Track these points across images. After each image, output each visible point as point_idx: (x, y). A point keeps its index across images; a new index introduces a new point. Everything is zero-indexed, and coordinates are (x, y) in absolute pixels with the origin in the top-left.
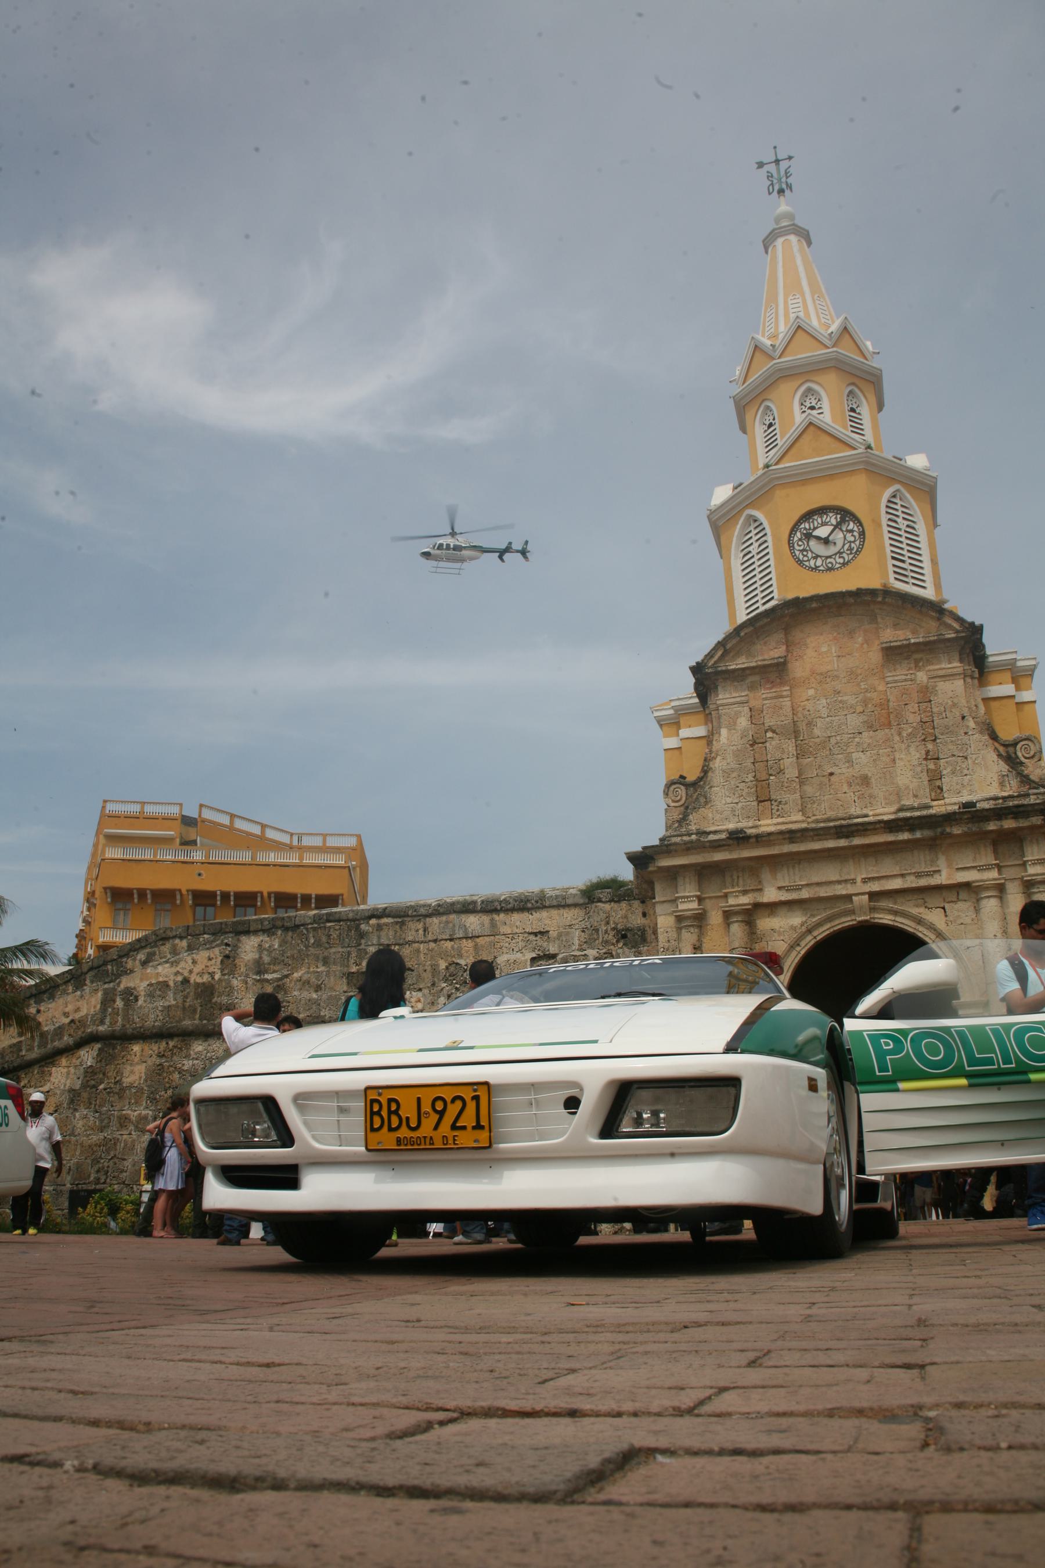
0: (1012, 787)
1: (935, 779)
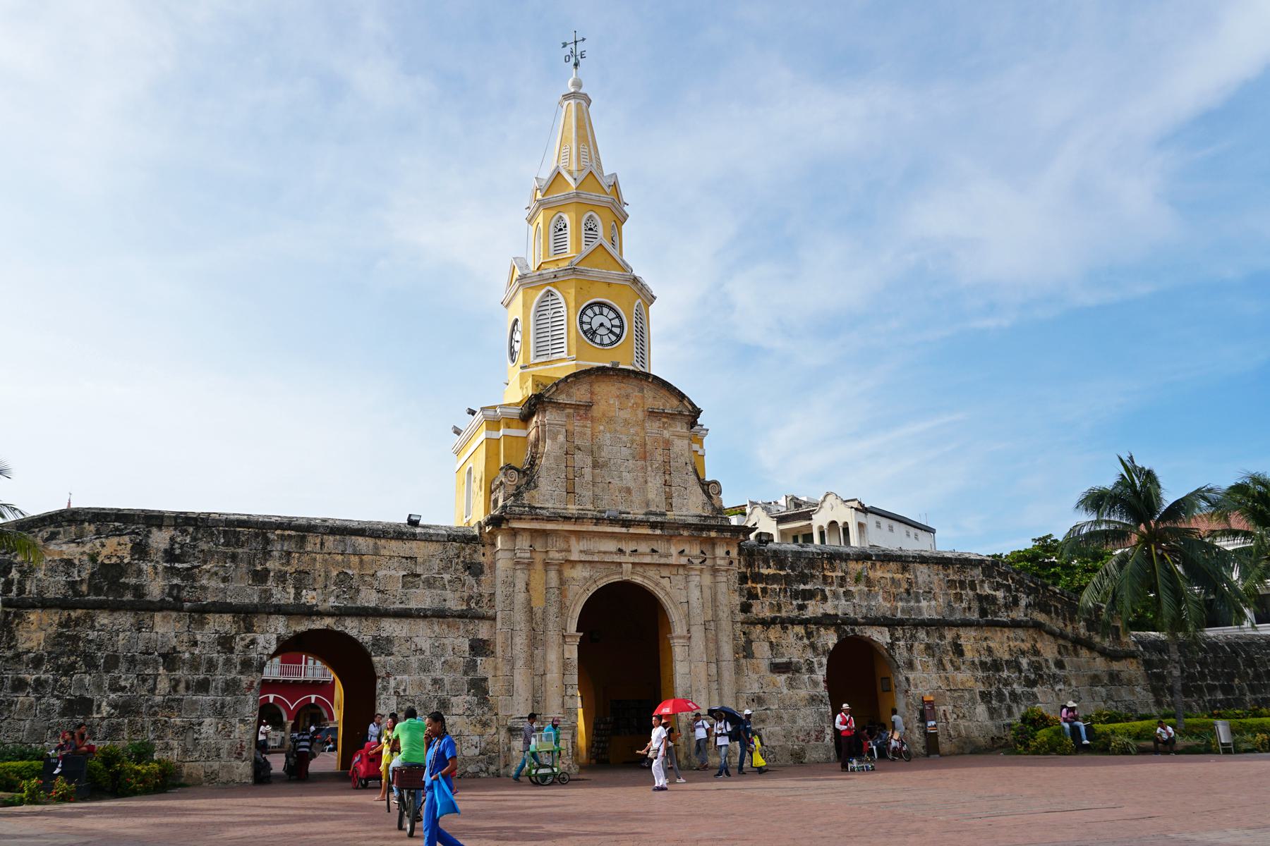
0: (707, 512)
1: (669, 497)
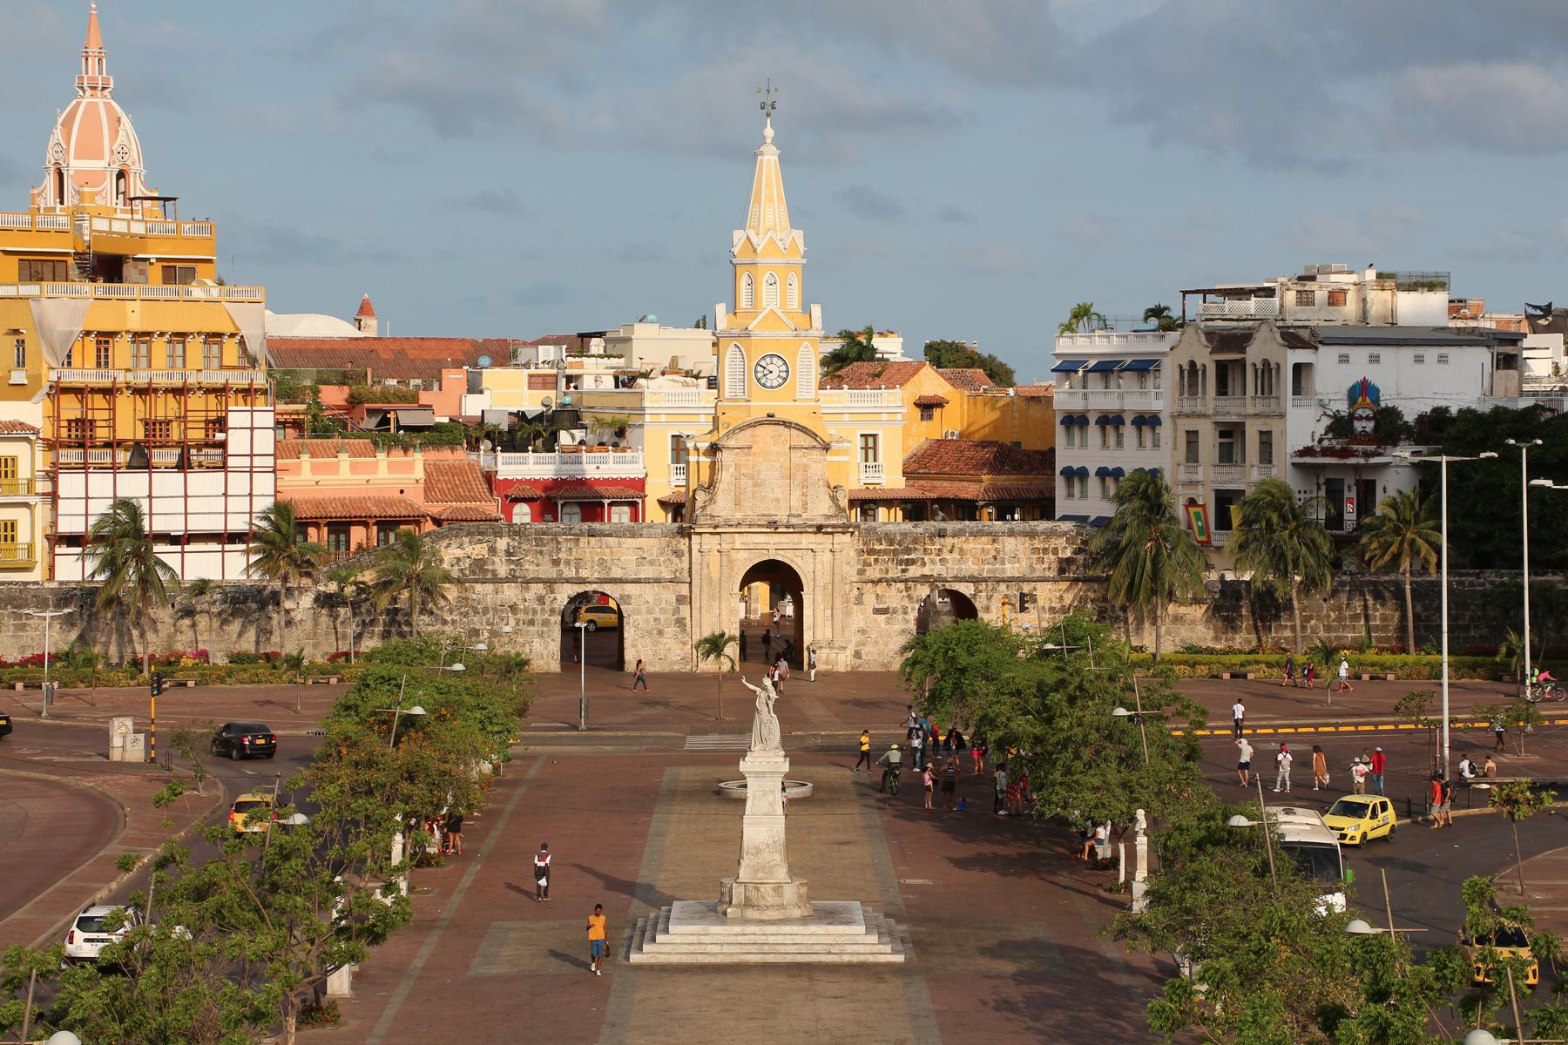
1: (805, 504)
